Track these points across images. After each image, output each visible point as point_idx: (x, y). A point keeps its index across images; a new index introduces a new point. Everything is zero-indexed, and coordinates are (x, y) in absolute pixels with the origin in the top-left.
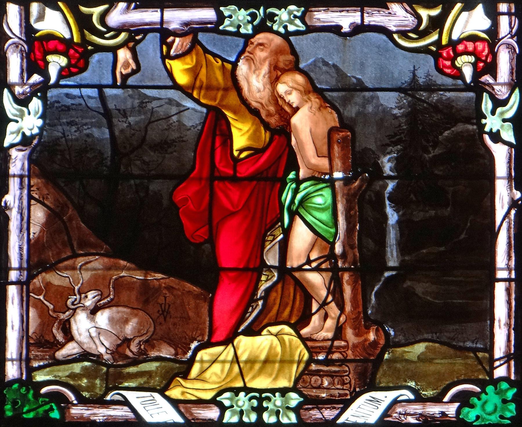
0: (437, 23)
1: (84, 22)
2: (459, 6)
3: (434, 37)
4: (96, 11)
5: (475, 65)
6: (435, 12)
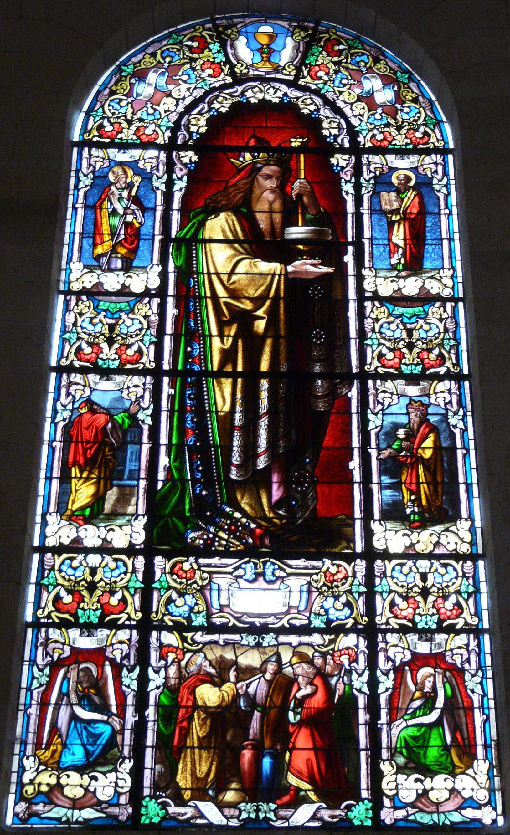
0: (332, 642)
2: (342, 635)
4: (190, 635)
6: (333, 637)
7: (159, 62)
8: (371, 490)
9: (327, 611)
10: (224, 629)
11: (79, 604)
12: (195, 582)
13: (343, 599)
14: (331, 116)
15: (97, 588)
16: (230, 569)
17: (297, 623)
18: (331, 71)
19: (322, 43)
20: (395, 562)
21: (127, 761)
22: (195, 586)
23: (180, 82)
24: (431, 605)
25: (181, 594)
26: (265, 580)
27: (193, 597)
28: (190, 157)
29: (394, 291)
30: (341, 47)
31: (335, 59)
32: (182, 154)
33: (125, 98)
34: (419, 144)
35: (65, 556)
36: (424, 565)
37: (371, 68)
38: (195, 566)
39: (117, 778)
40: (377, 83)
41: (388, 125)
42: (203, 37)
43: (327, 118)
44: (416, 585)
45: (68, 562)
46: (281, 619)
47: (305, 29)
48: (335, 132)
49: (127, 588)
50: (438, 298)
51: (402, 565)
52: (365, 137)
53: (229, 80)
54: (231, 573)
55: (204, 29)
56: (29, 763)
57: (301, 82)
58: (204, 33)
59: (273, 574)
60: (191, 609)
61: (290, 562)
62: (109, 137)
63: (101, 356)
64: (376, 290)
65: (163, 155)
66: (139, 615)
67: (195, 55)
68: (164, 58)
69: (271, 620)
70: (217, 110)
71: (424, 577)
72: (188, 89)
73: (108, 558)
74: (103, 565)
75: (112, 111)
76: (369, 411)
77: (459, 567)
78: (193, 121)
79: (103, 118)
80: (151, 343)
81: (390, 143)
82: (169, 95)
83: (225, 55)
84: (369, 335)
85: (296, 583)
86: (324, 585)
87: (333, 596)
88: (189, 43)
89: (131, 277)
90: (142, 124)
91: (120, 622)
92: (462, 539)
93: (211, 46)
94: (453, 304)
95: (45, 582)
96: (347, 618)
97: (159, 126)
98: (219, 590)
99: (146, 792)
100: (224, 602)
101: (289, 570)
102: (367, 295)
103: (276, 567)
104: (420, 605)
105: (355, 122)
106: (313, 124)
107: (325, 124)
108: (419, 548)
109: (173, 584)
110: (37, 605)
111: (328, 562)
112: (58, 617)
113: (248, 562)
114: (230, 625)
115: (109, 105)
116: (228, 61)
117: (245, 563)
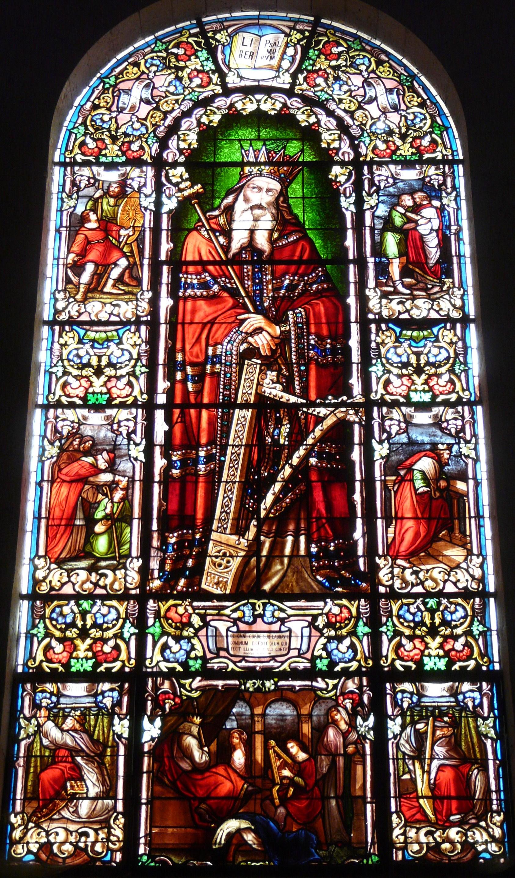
7: (143, 73)
30: (340, 49)
31: (334, 63)
37: (373, 71)
55: (191, 35)
58: (190, 40)
67: (182, 64)
68: (148, 68)
72: (177, 101)
79: (85, 135)
93: (199, 54)
106: (311, 135)
115: (92, 120)
116: (218, 70)
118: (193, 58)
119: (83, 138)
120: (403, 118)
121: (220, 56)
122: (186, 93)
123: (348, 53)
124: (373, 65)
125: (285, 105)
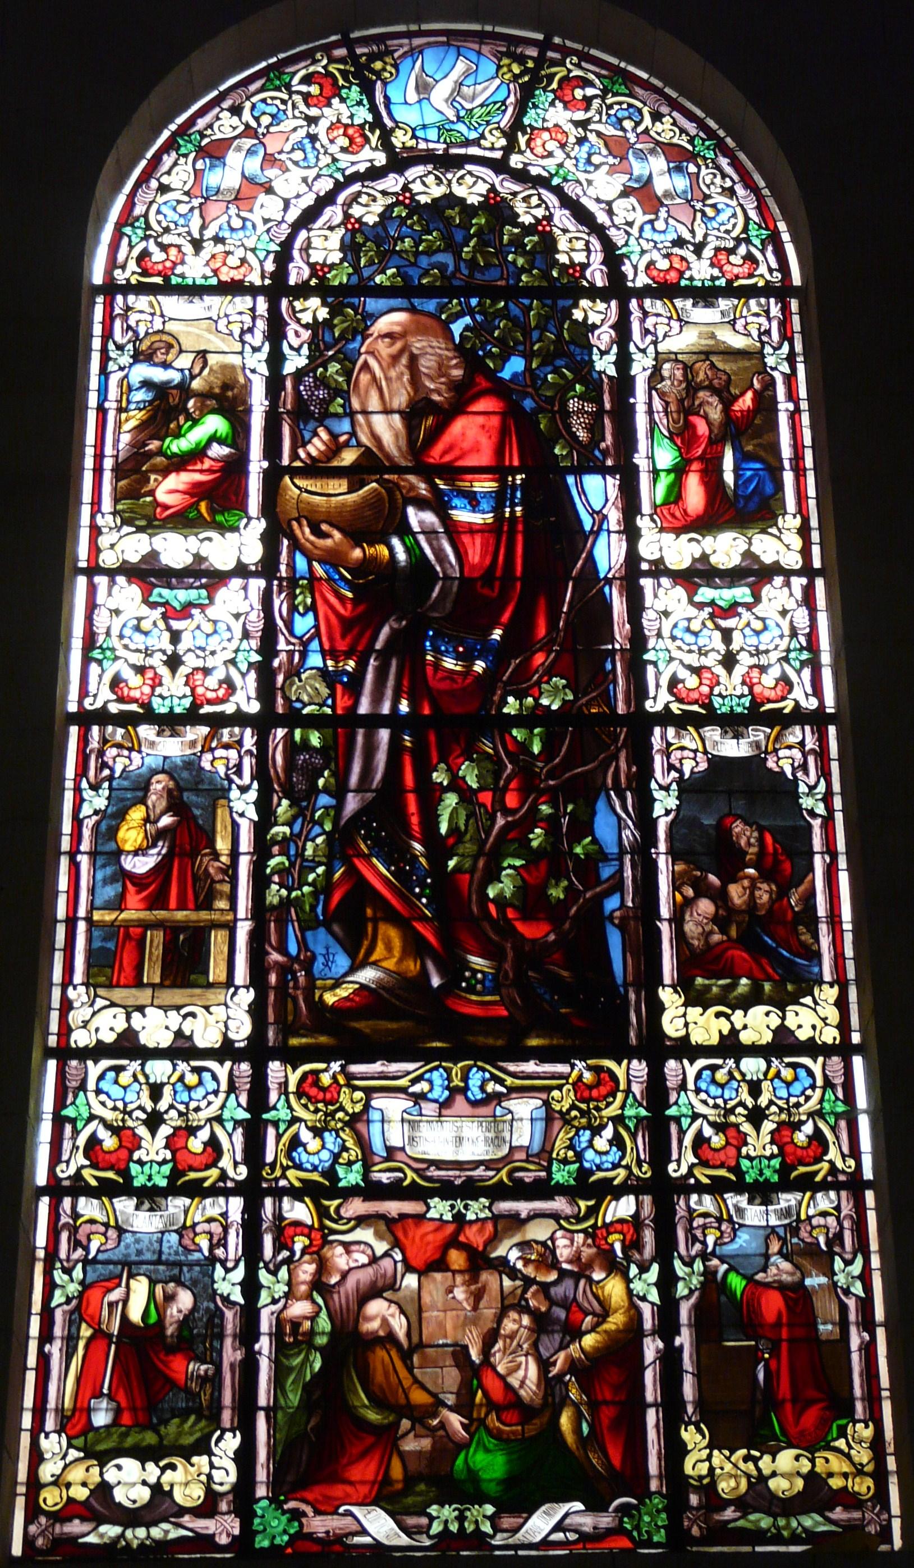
0: (592, 1211)
1: (322, 1213)
3: (591, 1222)
5: (623, 1242)
7: (247, 126)
8: (659, 931)
9: (579, 1156)
10: (395, 1191)
11: (131, 1153)
12: (342, 1108)
13: (608, 1132)
14: (572, 228)
15: (164, 1121)
16: (403, 1082)
17: (528, 1177)
18: (572, 140)
19: (554, 85)
20: (701, 1063)
21: (228, 1435)
22: (340, 1115)
23: (289, 164)
24: (768, 1139)
25: (317, 1132)
26: (467, 1099)
27: (338, 1136)
28: (314, 309)
29: (694, 560)
30: (590, 92)
31: (580, 115)
32: (298, 305)
33: (186, 199)
34: (737, 277)
35: (105, 1063)
36: (752, 1066)
37: (646, 131)
38: (342, 1080)
39: (212, 1466)
40: (658, 164)
41: (680, 242)
42: (329, 74)
43: (565, 231)
44: (742, 1104)
45: (111, 1075)
46: (499, 1170)
47: (521, 59)
48: (580, 257)
49: (219, 1119)
50: (776, 569)
51: (714, 1068)
52: (635, 268)
53: (381, 159)
54: (403, 1090)
55: (332, 60)
56: (51, 1444)
57: (515, 161)
59: (482, 1088)
60: (336, 1157)
61: (512, 1067)
62: (159, 274)
63: (158, 690)
64: (662, 558)
65: (262, 305)
66: (243, 1172)
68: (257, 119)
69: (480, 1172)
70: (359, 220)
71: (755, 1088)
73: (182, 1066)
74: (173, 1080)
75: (164, 224)
76: (653, 785)
77: (817, 1068)
78: (316, 242)
80: (251, 665)
81: (681, 274)
82: (269, 190)
83: (370, 110)
84: (652, 643)
85: (525, 1108)
86: (574, 1106)
87: (589, 1127)
88: (304, 88)
89: (209, 539)
90: (220, 248)
91: (206, 1184)
92: (824, 1020)
94: (804, 581)
95: (69, 1112)
96: (615, 1166)
97: (253, 250)
98: (383, 1121)
99: (261, 1491)
100: (396, 1141)
101: (509, 1081)
102: (645, 566)
103: (487, 1075)
104: (749, 1140)
105: (617, 237)
107: (563, 245)
108: (746, 1038)
109: (301, 1113)
110: (56, 1157)
111: (580, 1065)
112: (96, 1178)
113: (436, 1068)
114: (406, 1183)
115: (158, 212)
116: (377, 123)
117: (431, 1071)
118: (335, 101)
119: (144, 244)
120: (699, 215)
121: (379, 99)
122: (321, 164)
123: (603, 100)
124: (647, 121)
125: (493, 189)
